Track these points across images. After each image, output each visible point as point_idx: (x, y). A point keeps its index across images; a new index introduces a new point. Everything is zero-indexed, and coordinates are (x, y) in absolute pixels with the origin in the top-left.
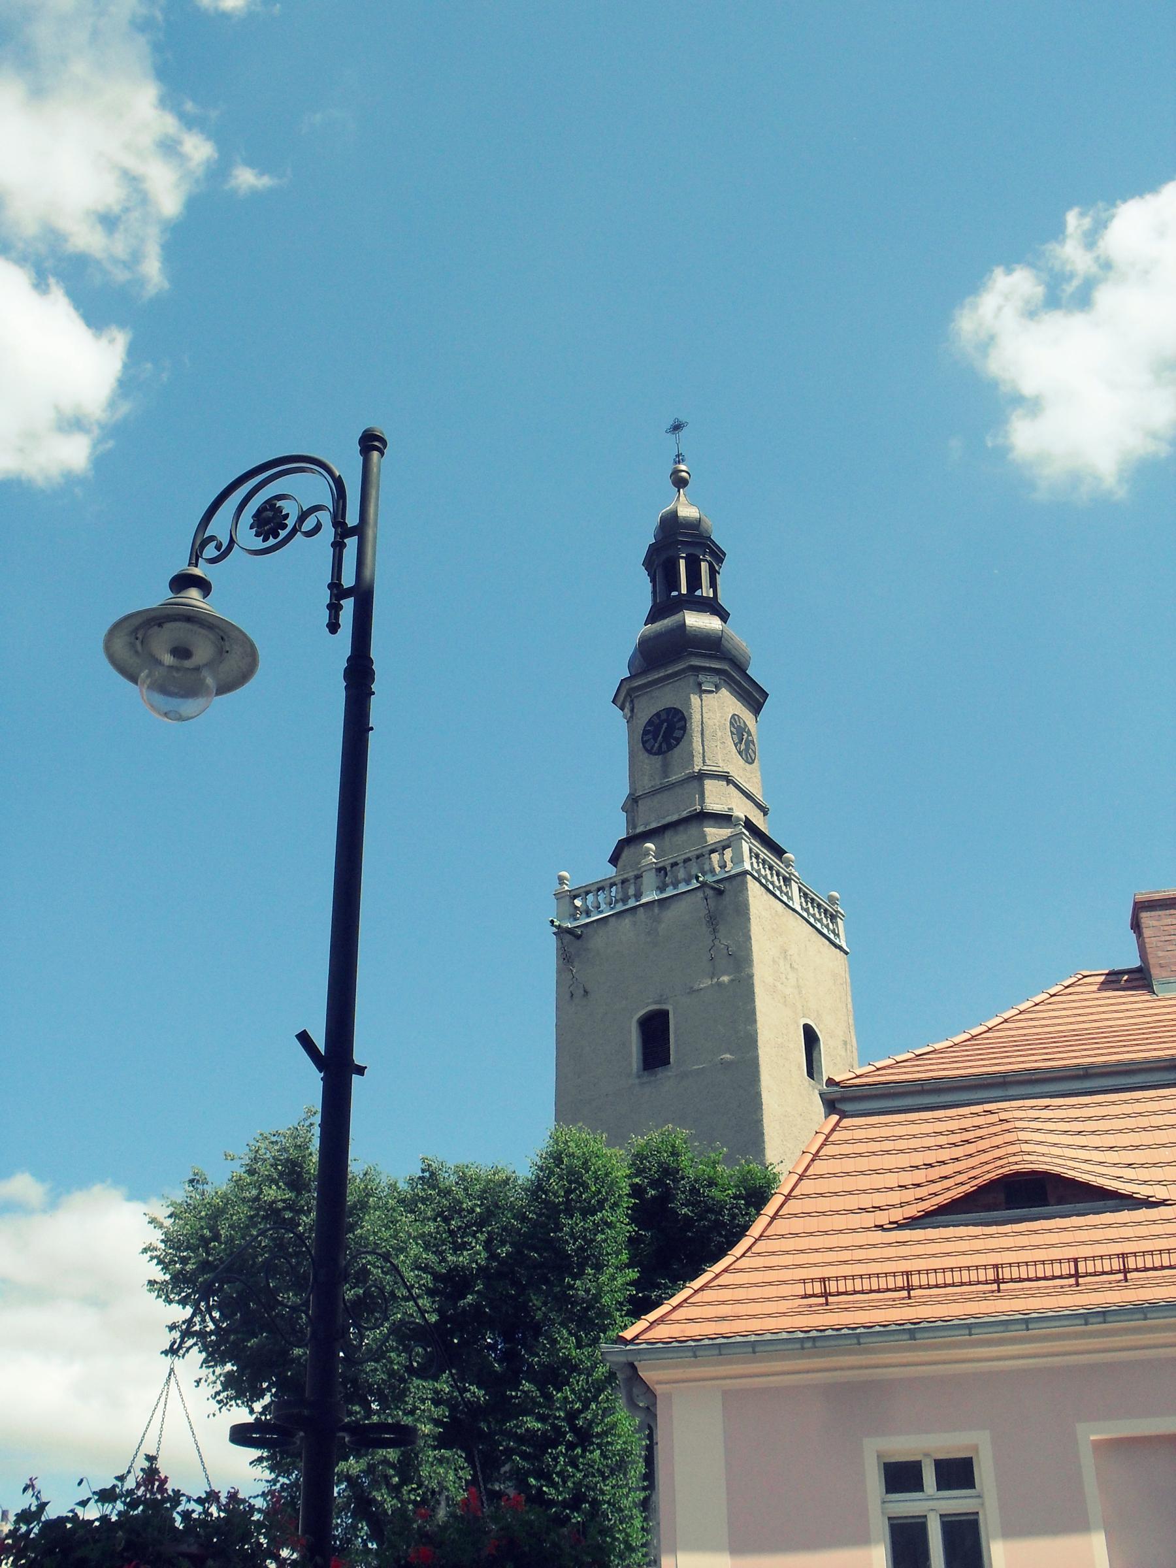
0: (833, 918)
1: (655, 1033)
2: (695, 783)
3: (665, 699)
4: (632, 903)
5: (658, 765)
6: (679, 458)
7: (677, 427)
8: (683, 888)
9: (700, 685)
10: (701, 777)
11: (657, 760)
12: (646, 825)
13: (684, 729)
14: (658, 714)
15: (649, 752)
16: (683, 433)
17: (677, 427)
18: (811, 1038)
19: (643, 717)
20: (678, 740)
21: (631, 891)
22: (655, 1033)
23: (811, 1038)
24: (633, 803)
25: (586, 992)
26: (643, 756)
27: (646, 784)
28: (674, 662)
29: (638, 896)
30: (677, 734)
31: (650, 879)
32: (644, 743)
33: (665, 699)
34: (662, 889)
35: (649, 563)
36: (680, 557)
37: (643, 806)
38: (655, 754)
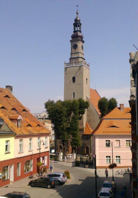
0: (89, 66)
1: (74, 79)
4: (72, 66)
6: (77, 10)
7: (77, 6)
8: (77, 65)
10: (78, 53)
11: (74, 50)
16: (78, 7)
17: (77, 6)
18: (87, 79)
19: (73, 44)
22: (74, 79)
26: (73, 49)
28: (76, 38)
36: (77, 24)
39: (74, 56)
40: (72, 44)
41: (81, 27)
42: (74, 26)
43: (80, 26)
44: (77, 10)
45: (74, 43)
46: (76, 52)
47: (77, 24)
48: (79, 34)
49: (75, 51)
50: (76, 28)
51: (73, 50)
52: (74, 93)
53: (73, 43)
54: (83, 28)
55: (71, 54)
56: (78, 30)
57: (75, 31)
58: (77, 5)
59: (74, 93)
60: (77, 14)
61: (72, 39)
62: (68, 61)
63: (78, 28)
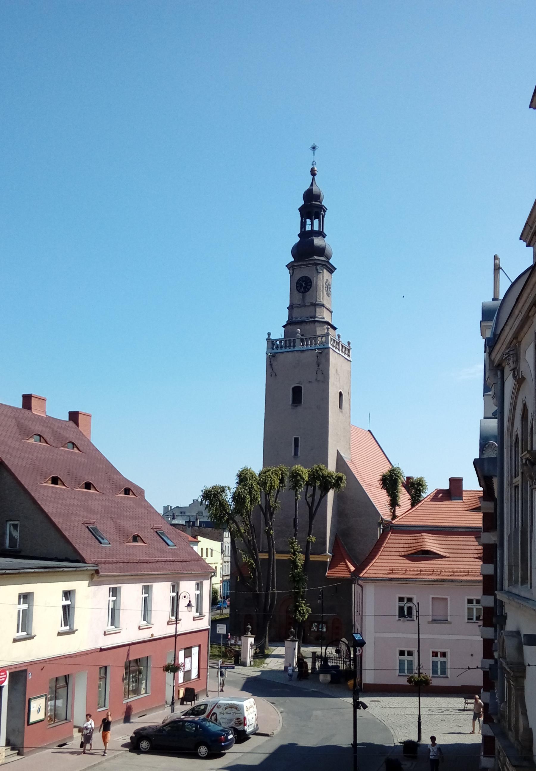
1: (297, 392)
2: (313, 307)
3: (304, 272)
4: (292, 349)
5: (301, 297)
6: (314, 163)
7: (314, 148)
9: (317, 270)
11: (301, 295)
12: (296, 318)
13: (311, 286)
14: (302, 277)
15: (298, 291)
16: (316, 151)
17: (314, 148)
20: (309, 290)
21: (292, 344)
22: (297, 392)
23: (341, 394)
24: (291, 308)
25: (276, 375)
26: (296, 292)
27: (297, 301)
28: (309, 257)
29: (294, 346)
30: (309, 287)
32: (297, 287)
33: (304, 272)
35: (300, 209)
37: (295, 310)
38: (300, 292)
39: (299, 314)
41: (324, 219)
42: (302, 217)
43: (323, 217)
44: (314, 163)
45: (300, 274)
47: (312, 207)
48: (317, 241)
49: (303, 298)
50: (308, 221)
52: (296, 440)
54: (331, 222)
56: (316, 228)
58: (311, 146)
59: (296, 440)
60: (313, 173)
62: (279, 334)
63: (316, 222)
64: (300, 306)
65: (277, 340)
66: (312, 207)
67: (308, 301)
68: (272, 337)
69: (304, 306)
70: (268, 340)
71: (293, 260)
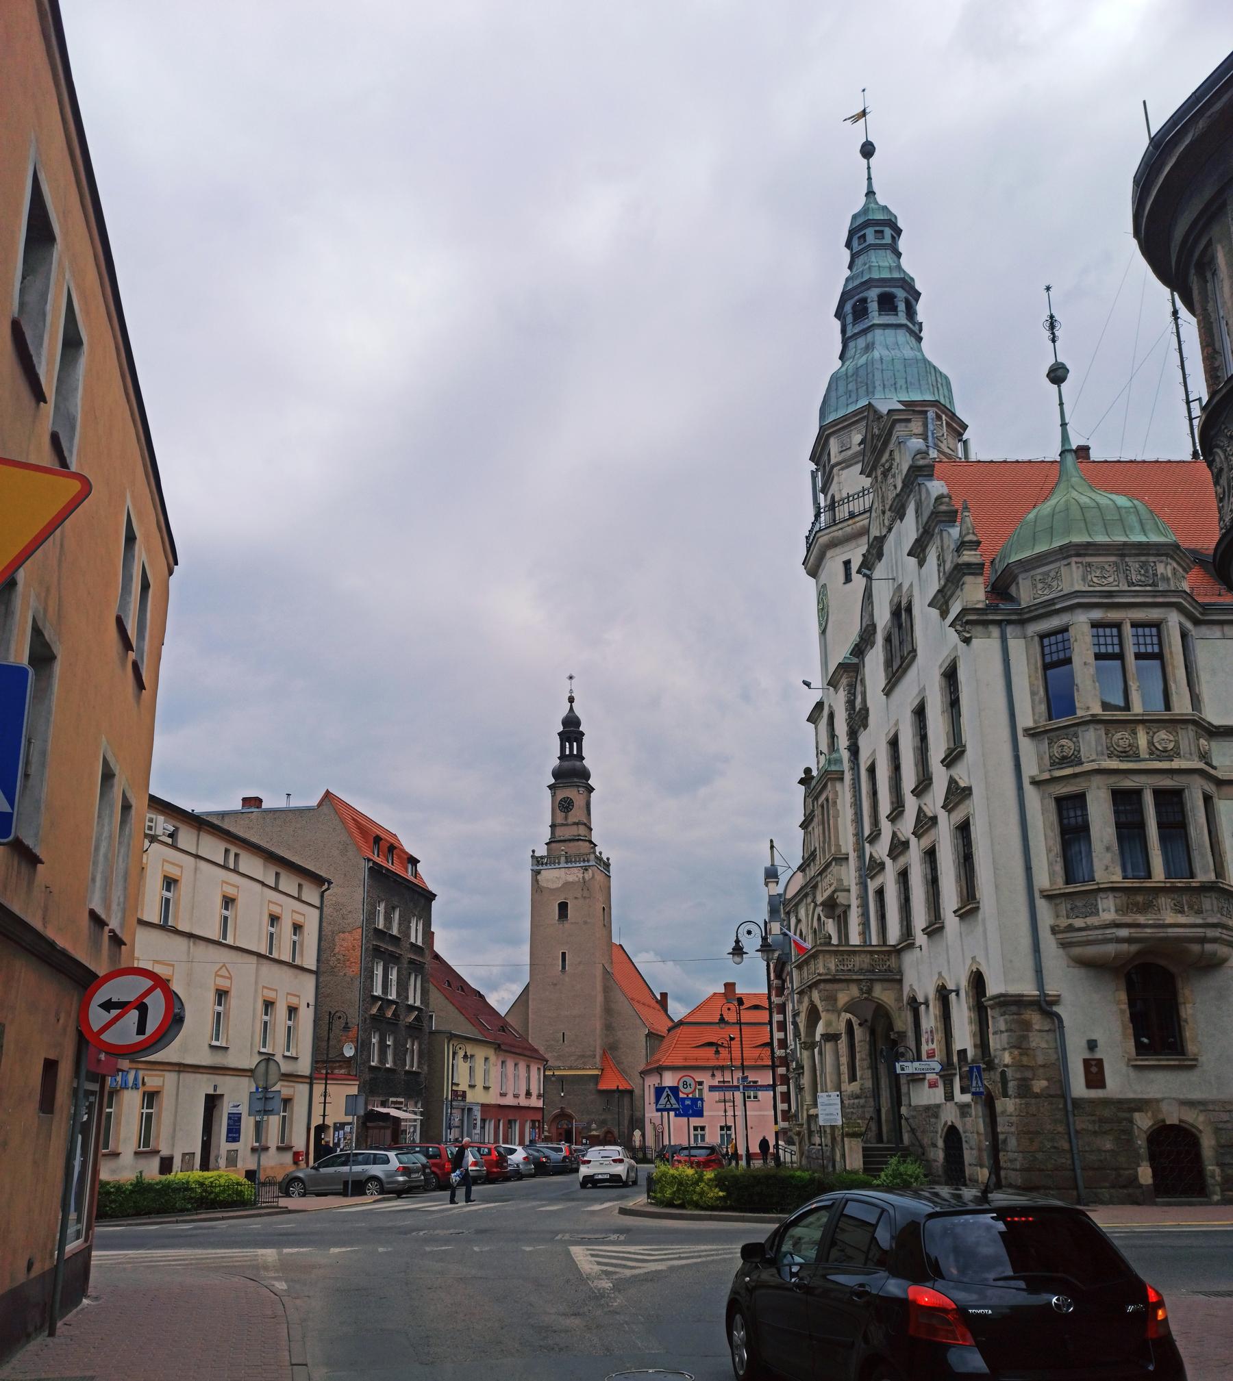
1: (563, 907)
6: (571, 691)
7: (571, 678)
17: (571, 678)
22: (563, 907)
31: (563, 859)
34: (567, 862)
40: (553, 796)
44: (571, 691)
45: (561, 794)
46: (570, 820)
49: (566, 818)
51: (560, 817)
53: (558, 792)
55: (553, 826)
57: (562, 757)
60: (571, 700)
61: (553, 781)
62: (542, 851)
64: (563, 825)
65: (542, 857)
66: (571, 731)
67: (570, 820)
68: (537, 854)
69: (567, 825)
70: (533, 857)
71: (553, 781)
